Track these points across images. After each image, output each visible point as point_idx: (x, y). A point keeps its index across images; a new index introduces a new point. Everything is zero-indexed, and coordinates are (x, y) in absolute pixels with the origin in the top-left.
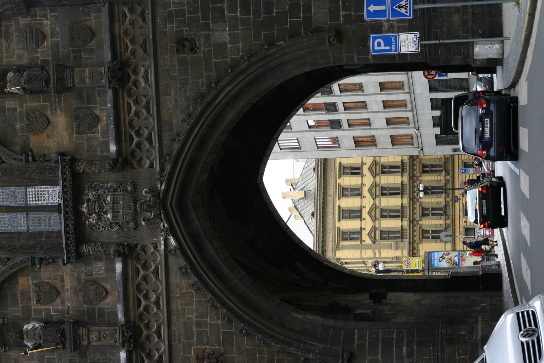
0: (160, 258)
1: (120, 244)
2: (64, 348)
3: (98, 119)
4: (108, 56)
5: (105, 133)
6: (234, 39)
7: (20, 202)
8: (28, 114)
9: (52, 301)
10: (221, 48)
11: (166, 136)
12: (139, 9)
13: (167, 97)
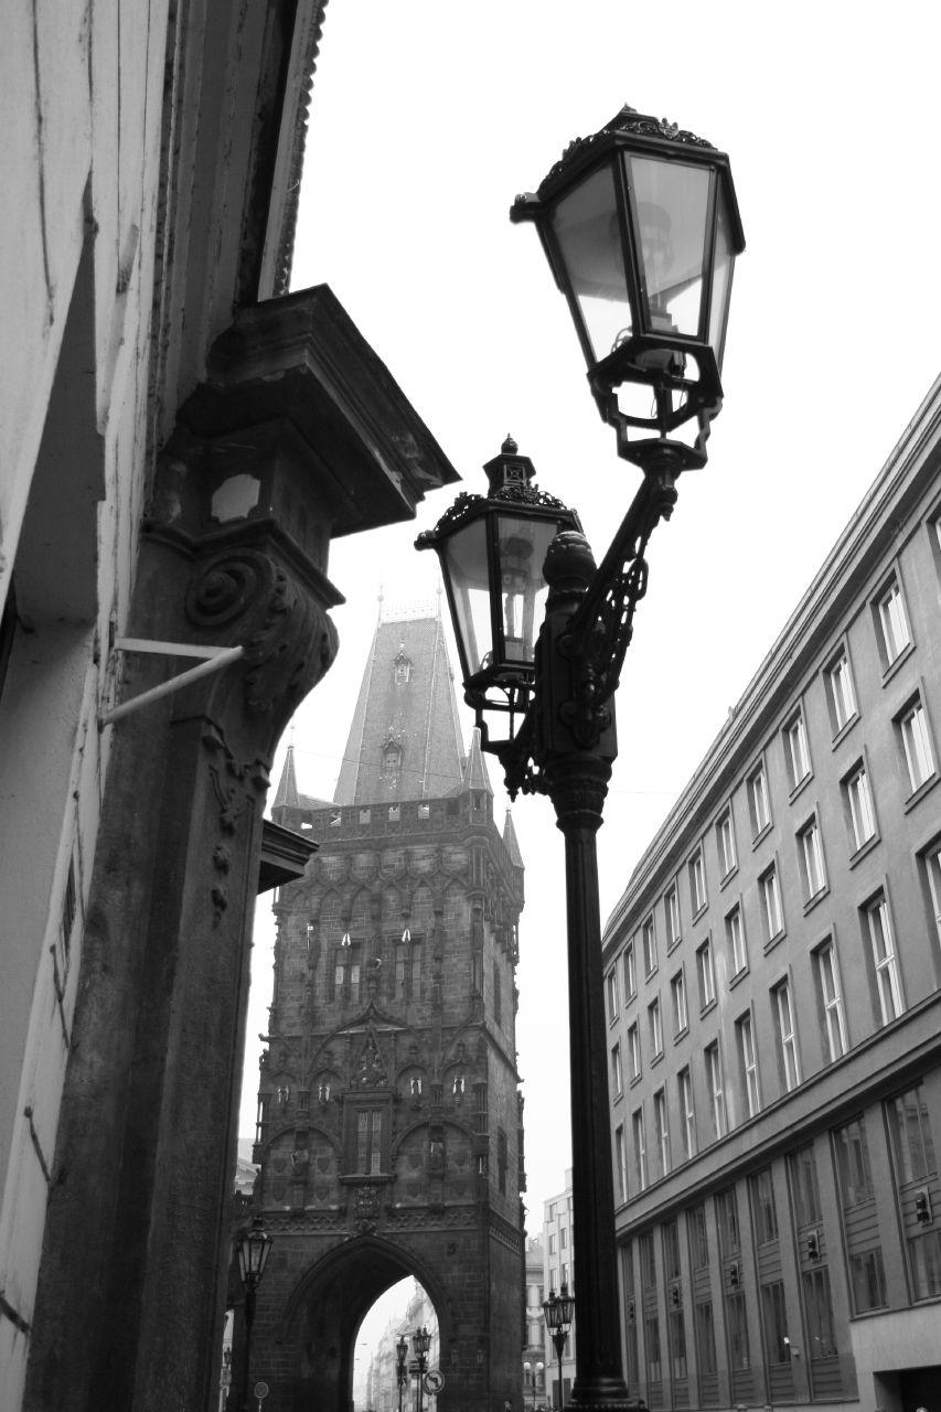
0: (339, 1232)
1: (346, 1209)
3: (415, 1196)
4: (446, 1204)
5: (406, 1201)
7: (374, 1149)
9: (321, 1168)
11: (403, 1237)
12: (473, 1221)
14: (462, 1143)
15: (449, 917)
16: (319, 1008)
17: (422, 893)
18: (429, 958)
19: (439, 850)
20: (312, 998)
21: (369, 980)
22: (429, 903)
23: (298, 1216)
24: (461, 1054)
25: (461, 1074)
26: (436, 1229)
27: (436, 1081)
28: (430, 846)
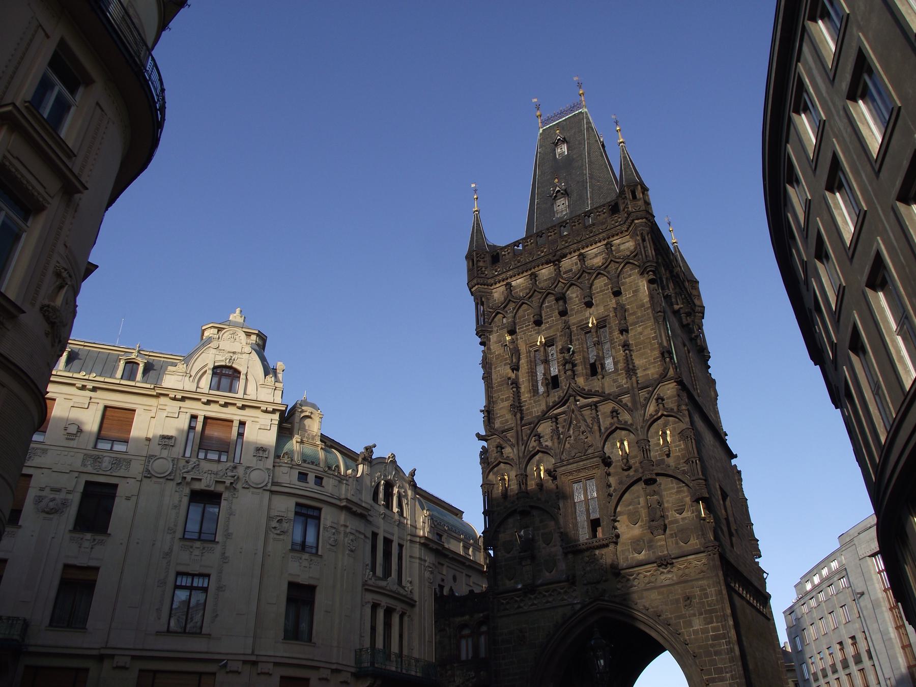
2: (520, 553)
6: (696, 632)
8: (637, 512)
10: (689, 624)
13: (657, 594)
14: (678, 492)
15: (627, 295)
16: (526, 401)
17: (600, 283)
18: (616, 334)
19: (609, 246)
20: (517, 394)
21: (565, 365)
22: (608, 289)
23: (530, 590)
24: (661, 406)
25: (665, 425)
26: (667, 582)
27: (641, 437)
28: (599, 244)
